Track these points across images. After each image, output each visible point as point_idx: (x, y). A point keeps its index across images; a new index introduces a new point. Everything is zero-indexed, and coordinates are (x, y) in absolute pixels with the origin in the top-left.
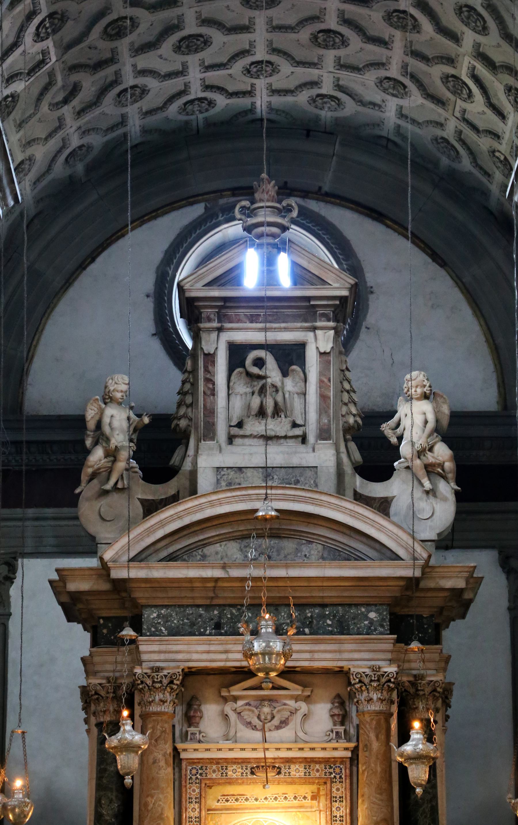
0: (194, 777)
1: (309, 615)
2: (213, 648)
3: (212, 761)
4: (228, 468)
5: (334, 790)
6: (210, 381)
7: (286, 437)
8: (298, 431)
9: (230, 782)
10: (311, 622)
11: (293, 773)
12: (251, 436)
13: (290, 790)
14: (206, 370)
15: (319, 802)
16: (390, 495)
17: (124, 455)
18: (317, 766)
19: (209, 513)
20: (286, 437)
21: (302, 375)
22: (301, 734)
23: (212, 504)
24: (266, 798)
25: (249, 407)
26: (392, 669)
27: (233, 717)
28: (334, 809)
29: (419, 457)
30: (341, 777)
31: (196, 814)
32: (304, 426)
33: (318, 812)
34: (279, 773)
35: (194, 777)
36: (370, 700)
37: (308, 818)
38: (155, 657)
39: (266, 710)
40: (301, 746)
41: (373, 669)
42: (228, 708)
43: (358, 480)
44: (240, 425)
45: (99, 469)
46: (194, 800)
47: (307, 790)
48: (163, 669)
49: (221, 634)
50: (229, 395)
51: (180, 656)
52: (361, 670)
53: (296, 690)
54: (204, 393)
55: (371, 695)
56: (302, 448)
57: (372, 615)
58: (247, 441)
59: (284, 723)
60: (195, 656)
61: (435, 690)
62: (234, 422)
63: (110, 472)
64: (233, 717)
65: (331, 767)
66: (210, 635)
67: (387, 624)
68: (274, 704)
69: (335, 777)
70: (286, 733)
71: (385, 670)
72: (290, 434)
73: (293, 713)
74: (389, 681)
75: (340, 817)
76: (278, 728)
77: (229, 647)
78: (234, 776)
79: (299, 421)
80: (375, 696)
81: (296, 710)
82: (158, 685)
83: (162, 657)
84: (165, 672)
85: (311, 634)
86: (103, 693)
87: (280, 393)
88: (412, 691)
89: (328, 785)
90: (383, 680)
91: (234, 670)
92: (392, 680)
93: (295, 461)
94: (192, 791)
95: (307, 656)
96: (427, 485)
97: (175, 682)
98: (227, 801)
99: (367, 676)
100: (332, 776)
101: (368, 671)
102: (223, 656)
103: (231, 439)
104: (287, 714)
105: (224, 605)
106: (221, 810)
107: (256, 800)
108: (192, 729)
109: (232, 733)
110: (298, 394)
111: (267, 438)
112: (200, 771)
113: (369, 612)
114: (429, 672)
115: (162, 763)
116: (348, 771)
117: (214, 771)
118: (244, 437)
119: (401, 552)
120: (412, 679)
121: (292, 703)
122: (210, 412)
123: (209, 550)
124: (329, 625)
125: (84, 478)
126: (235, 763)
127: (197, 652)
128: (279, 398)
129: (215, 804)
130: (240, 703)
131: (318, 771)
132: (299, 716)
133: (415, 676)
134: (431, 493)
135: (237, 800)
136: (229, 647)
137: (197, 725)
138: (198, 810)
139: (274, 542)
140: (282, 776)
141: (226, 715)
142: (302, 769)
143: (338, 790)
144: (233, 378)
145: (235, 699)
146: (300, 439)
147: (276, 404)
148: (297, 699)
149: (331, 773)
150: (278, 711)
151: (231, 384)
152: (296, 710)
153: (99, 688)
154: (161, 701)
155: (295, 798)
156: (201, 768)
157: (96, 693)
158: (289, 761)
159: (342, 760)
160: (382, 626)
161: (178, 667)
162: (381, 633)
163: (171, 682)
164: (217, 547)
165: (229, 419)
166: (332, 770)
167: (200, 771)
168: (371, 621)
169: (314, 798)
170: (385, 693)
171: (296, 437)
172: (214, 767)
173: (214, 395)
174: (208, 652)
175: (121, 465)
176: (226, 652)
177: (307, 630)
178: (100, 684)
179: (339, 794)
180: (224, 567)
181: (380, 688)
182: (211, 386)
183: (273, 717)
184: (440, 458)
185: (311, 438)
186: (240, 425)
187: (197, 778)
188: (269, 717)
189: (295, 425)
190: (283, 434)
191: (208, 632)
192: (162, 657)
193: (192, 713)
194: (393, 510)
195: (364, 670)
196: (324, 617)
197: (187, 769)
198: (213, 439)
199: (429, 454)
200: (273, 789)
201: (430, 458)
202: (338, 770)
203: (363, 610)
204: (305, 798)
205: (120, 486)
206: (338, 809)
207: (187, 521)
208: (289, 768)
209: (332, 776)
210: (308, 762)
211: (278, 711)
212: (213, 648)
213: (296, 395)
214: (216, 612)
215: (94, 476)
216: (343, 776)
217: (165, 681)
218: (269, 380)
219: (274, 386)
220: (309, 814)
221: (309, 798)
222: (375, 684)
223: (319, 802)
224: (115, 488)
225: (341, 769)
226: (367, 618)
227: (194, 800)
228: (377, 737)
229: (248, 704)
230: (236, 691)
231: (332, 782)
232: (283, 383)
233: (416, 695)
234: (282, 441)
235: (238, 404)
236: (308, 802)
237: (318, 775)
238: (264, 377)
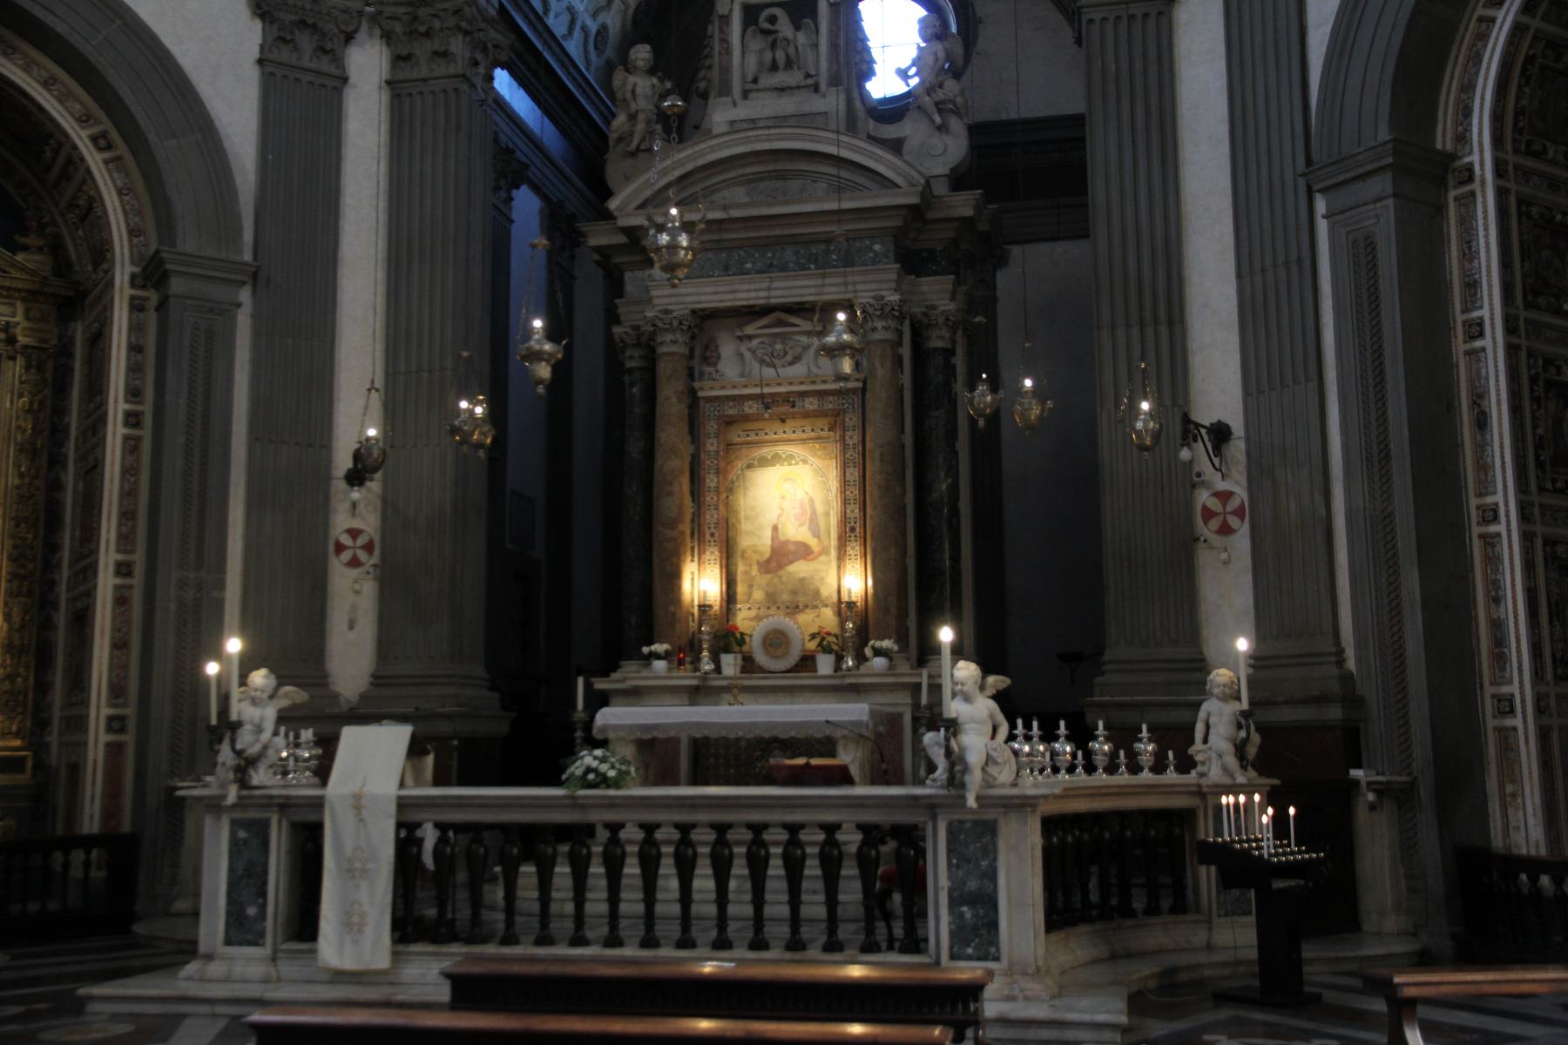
0: (712, 414)
1: (815, 251)
2: (720, 289)
3: (728, 398)
4: (742, 121)
5: (847, 420)
6: (725, 41)
7: (798, 87)
8: (810, 81)
9: (747, 418)
10: (816, 259)
11: (807, 406)
12: (765, 90)
13: (807, 423)
14: (721, 31)
15: (835, 433)
16: (904, 135)
17: (641, 117)
18: (831, 398)
19: (712, 157)
20: (798, 87)
21: (812, 26)
22: (814, 369)
23: (712, 149)
24: (785, 432)
25: (761, 63)
26: (895, 298)
27: (748, 355)
28: (847, 438)
29: (929, 95)
30: (853, 408)
31: (714, 448)
32: (817, 75)
33: (834, 443)
34: (793, 406)
35: (712, 414)
36: (874, 329)
37: (825, 448)
38: (665, 300)
39: (778, 347)
40: (812, 379)
41: (876, 298)
42: (743, 349)
43: (871, 123)
44: (755, 81)
45: (623, 133)
46: (712, 435)
47: (823, 423)
48: (671, 311)
49: (729, 275)
50: (743, 53)
51: (689, 299)
52: (864, 301)
53: (806, 325)
54: (720, 53)
55: (875, 324)
56: (814, 96)
57: (877, 247)
58: (761, 95)
59: (797, 359)
60: (704, 298)
61: (948, 319)
62: (750, 78)
63: (632, 134)
64: (748, 355)
65: (844, 399)
66: (718, 276)
67: (891, 255)
68: (787, 341)
69: (848, 408)
70: (799, 369)
71: (888, 299)
72: (802, 84)
73: (806, 348)
74: (893, 309)
75: (854, 444)
76: (791, 364)
77: (737, 287)
78: (750, 411)
79: (812, 72)
80: (879, 324)
81: (809, 346)
82: (667, 326)
83: (673, 300)
84: (675, 314)
85: (816, 269)
86: (629, 342)
87: (792, 46)
88: (925, 321)
89: (842, 416)
90: (887, 309)
91: (747, 310)
92: (896, 308)
93: (806, 109)
94: (711, 426)
95: (812, 291)
96: (938, 119)
97: (684, 322)
98: (748, 436)
99: (871, 305)
100: (845, 407)
101: (871, 301)
102: (730, 296)
103: (745, 95)
104: (799, 350)
105: (732, 248)
106: (742, 444)
107: (775, 434)
108: (708, 369)
109: (748, 369)
110: (810, 46)
111: (781, 90)
112: (718, 408)
113: (873, 244)
114: (941, 302)
115: (674, 400)
116: (860, 401)
117: (731, 408)
118: (758, 90)
119: (899, 180)
120: (924, 310)
121: (804, 339)
122: (726, 70)
123: (717, 197)
124: (834, 260)
125: (611, 143)
126: (751, 399)
127: (705, 294)
128: (791, 51)
129: (736, 440)
130: (755, 342)
131: (831, 402)
132: (812, 351)
133: (927, 307)
134: (942, 128)
135: (757, 435)
136: (737, 287)
137: (715, 365)
138: (716, 444)
139: (780, 183)
140: (796, 409)
141: (742, 354)
142: (816, 402)
143: (851, 419)
144: (746, 36)
145: (750, 338)
146: (812, 88)
147: (788, 56)
148: (809, 334)
149: (844, 404)
150: (791, 348)
151: (745, 42)
152: (809, 346)
153: (624, 336)
154: (671, 341)
155: (813, 430)
156: (719, 406)
157: (622, 341)
158: (803, 394)
159: (854, 391)
160: (887, 257)
161: (686, 309)
162: (886, 264)
163: (681, 323)
164: (725, 193)
165: (744, 77)
166: (845, 401)
167: (718, 408)
168: (876, 254)
169: (829, 430)
170: (890, 322)
171: (807, 86)
172: (731, 404)
173: (728, 54)
174: (716, 293)
175: (640, 126)
176: (734, 292)
177: (812, 266)
178: (625, 333)
179: (852, 423)
180: (725, 208)
181: (882, 317)
182: (725, 45)
183: (786, 354)
184: (950, 94)
185: (823, 87)
186: (755, 81)
187: (715, 415)
188: (782, 353)
189: (808, 76)
190: (794, 85)
191: (717, 274)
192: (673, 300)
193: (708, 354)
194: (906, 149)
195: (868, 300)
196: (828, 252)
197: (706, 408)
198: (727, 95)
199: (940, 91)
200: (790, 423)
201: (940, 95)
202: (850, 401)
203: (868, 242)
204: (822, 430)
205: (643, 147)
206: (851, 437)
207: (689, 167)
208: (803, 401)
209: (845, 407)
210: (821, 394)
211: (791, 348)
212: (720, 289)
213: (809, 48)
214: (724, 255)
215: (620, 140)
216: (856, 406)
217: (675, 323)
218: (781, 35)
219: (786, 39)
220: (826, 445)
221: (826, 429)
222: (878, 313)
223: (835, 433)
224: (638, 149)
225: (854, 400)
226: (872, 250)
227: (712, 435)
228: (882, 366)
229: (763, 343)
230: (750, 330)
231: (845, 412)
232: (795, 37)
233: (929, 326)
234: (795, 91)
235: (752, 60)
236: (825, 433)
237: (831, 406)
238: (776, 32)
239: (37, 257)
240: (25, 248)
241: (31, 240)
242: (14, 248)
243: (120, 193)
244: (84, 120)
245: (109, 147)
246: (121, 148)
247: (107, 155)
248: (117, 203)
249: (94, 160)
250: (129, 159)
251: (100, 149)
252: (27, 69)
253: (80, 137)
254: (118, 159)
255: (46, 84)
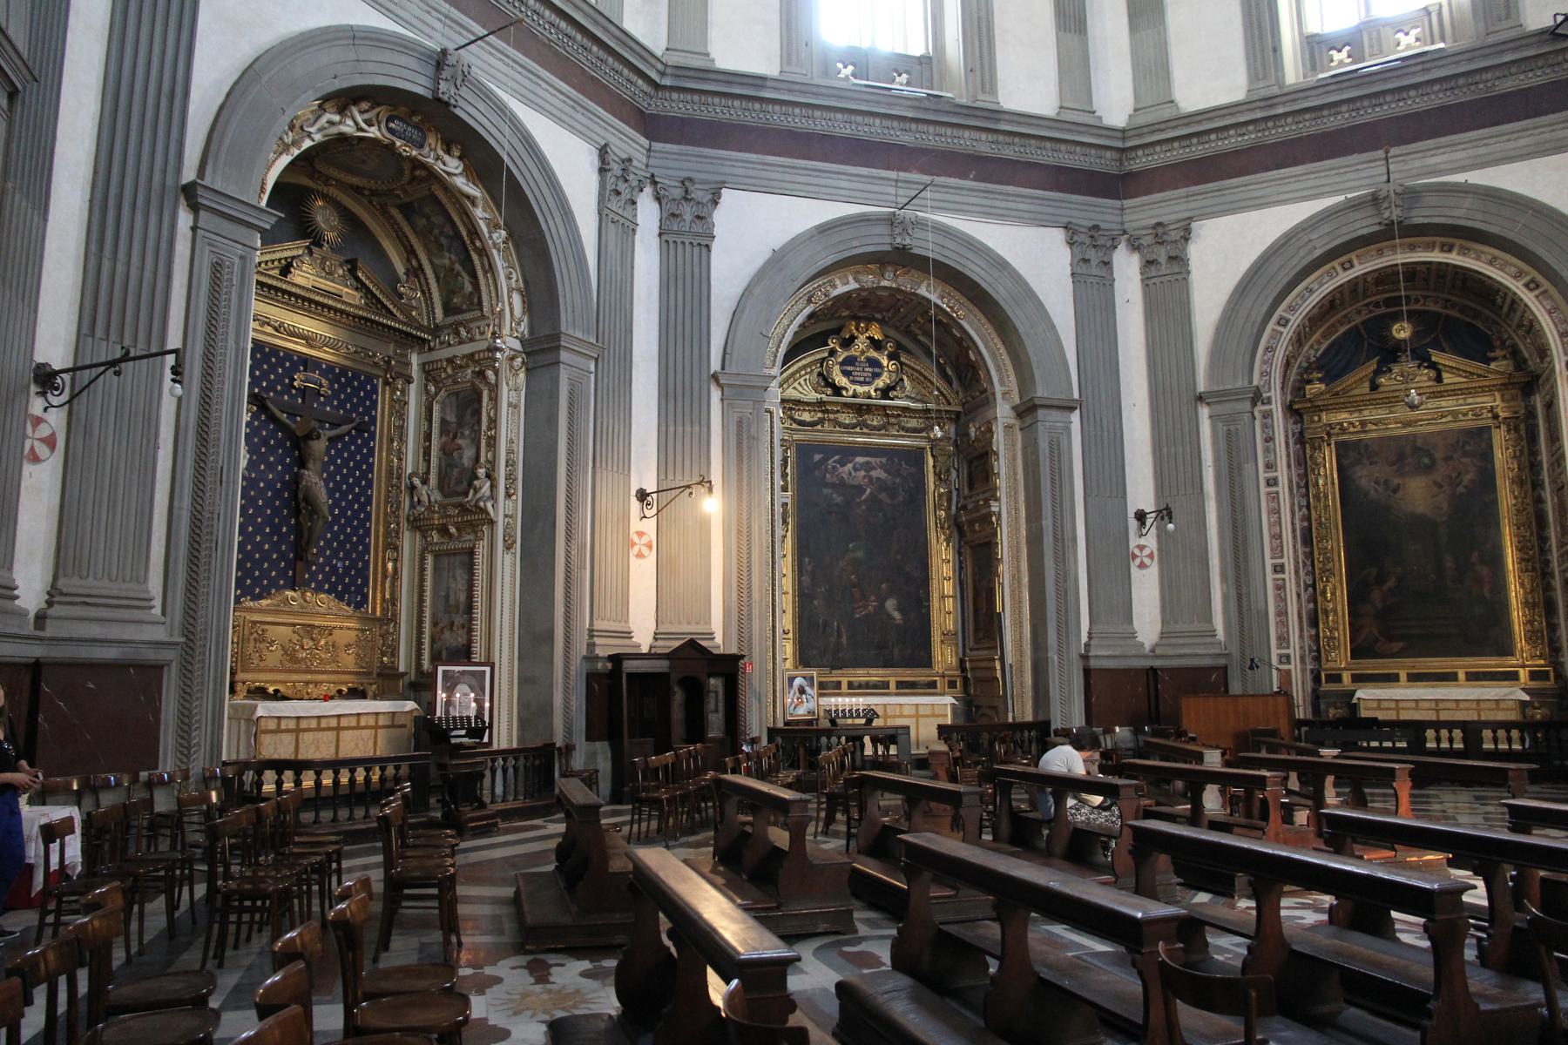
239: (1504, 362)
240: (1494, 359)
241: (1498, 353)
242: (1488, 361)
243: (1549, 313)
244: (1518, 276)
245: (1538, 286)
246: (1546, 285)
247: (1537, 292)
248: (1549, 320)
249: (1528, 298)
250: (1553, 291)
251: (1531, 290)
252: (1478, 259)
253: (1517, 287)
254: (1545, 292)
255: (1490, 263)
